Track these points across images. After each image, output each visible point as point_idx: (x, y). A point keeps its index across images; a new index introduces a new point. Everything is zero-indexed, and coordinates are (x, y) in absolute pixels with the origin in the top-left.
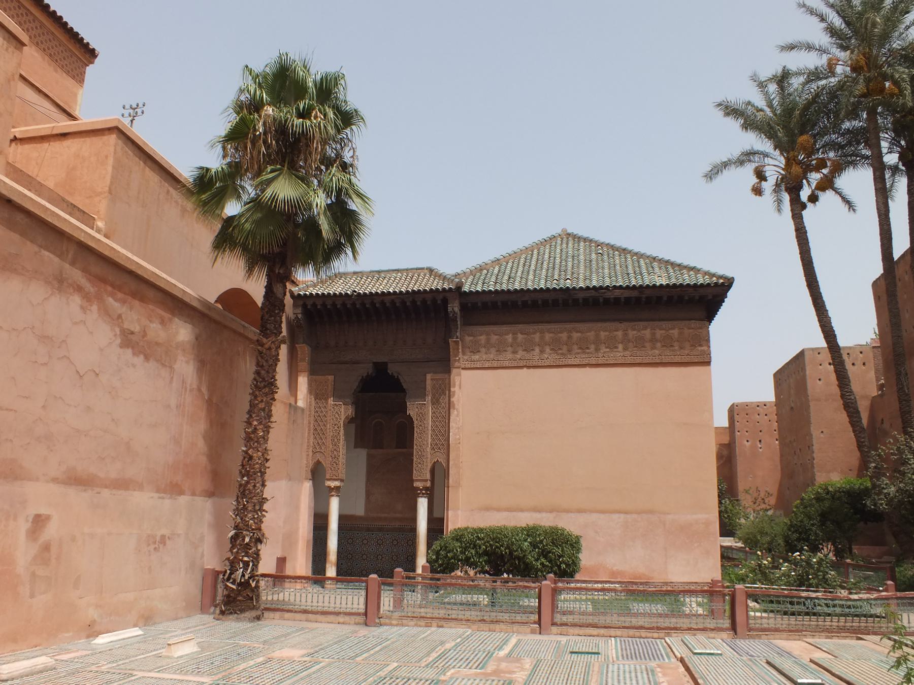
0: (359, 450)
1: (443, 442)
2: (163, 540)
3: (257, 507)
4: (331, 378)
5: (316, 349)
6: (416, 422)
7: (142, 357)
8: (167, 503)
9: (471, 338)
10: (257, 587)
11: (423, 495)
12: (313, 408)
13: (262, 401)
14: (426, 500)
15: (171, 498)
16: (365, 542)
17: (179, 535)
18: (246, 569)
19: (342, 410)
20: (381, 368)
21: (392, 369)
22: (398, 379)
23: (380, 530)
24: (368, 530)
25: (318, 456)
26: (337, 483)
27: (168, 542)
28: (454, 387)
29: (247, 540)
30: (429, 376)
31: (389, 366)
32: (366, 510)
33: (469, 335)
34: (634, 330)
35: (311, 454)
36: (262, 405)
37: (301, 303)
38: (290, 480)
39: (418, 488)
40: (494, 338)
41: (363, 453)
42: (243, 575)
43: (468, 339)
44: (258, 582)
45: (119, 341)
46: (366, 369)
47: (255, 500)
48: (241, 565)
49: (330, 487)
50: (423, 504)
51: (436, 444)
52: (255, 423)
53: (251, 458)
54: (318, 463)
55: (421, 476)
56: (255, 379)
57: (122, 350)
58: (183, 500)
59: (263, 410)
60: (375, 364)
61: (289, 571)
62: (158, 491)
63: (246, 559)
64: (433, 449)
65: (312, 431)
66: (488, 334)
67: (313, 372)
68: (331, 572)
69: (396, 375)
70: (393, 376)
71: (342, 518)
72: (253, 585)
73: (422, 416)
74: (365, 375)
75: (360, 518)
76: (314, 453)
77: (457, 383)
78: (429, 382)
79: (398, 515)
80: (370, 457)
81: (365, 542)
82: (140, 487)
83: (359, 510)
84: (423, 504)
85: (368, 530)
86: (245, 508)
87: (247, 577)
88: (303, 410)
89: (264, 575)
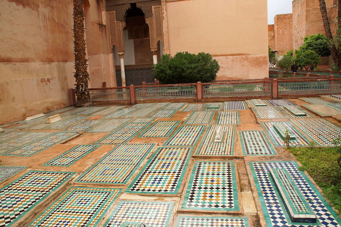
0: (130, 40)
1: (160, 33)
2: (48, 80)
3: (83, 63)
6: (149, 26)
7: (21, 6)
8: (47, 66)
10: (88, 94)
11: (155, 54)
12: (109, 25)
13: (78, 20)
14: (157, 56)
15: (49, 64)
16: (137, 74)
17: (55, 78)
18: (82, 87)
21: (138, 6)
22: (141, 10)
23: (142, 69)
24: (137, 70)
25: (114, 43)
26: (122, 53)
27: (51, 81)
28: (163, 10)
29: (81, 77)
30: (153, 7)
32: (136, 63)
36: (79, 22)
38: (103, 54)
39: (153, 52)
41: (132, 41)
42: (82, 90)
44: (88, 92)
46: (128, 7)
47: (82, 60)
48: (81, 86)
49: (119, 55)
51: (158, 34)
52: (77, 29)
53: (78, 44)
54: (114, 46)
55: (153, 48)
56: (74, 11)
57: (10, 3)
58: (54, 64)
59: (80, 24)
60: (131, 4)
61: (108, 86)
62: (42, 61)
63: (82, 84)
64: (157, 36)
65: (110, 34)
67: (107, 10)
69: (139, 8)
70: (138, 8)
71: (125, 66)
72: (86, 93)
74: (128, 9)
75: (134, 65)
76: (112, 42)
77: (165, 9)
78: (153, 9)
79: (148, 63)
80: (135, 42)
81: (137, 74)
82: (34, 61)
83: (133, 62)
85: (137, 70)
86: (78, 64)
87: (83, 91)
88: (105, 26)
89: (90, 89)
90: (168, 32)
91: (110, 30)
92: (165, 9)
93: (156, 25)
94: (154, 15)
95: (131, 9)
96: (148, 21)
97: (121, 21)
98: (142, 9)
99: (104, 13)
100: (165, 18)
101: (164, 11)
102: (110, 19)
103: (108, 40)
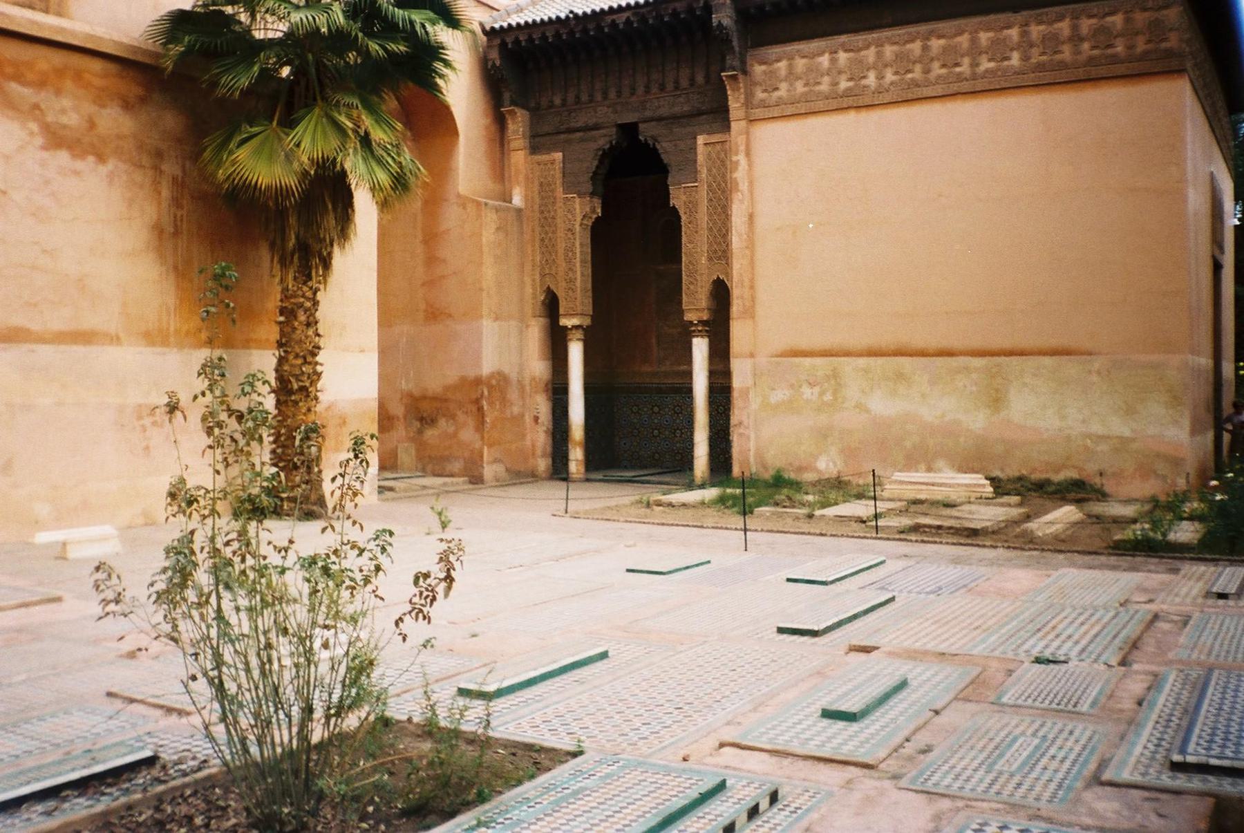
4: (558, 156)
5: (536, 114)
6: (684, 218)
7: (91, 159)
9: (763, 67)
11: (700, 334)
12: (536, 207)
19: (577, 206)
20: (629, 131)
21: (647, 132)
22: (655, 150)
25: (549, 282)
30: (701, 140)
31: (642, 127)
33: (762, 63)
34: (1040, 23)
35: (537, 277)
37: (497, 41)
38: (496, 319)
40: (800, 64)
43: (758, 69)
45: (39, 141)
50: (700, 348)
55: (696, 306)
57: (46, 154)
64: (710, 259)
66: (791, 58)
67: (534, 149)
68: (576, 455)
70: (646, 144)
73: (693, 206)
76: (543, 276)
81: (656, 409)
84: (700, 348)
90: (751, 245)
91: (538, 229)
92: (742, 148)
93: (710, 215)
94: (704, 174)
95: (625, 144)
96: (678, 199)
97: (580, 195)
98: (658, 147)
99: (519, 158)
100: (744, 186)
101: (741, 158)
102: (541, 184)
103: (528, 267)
